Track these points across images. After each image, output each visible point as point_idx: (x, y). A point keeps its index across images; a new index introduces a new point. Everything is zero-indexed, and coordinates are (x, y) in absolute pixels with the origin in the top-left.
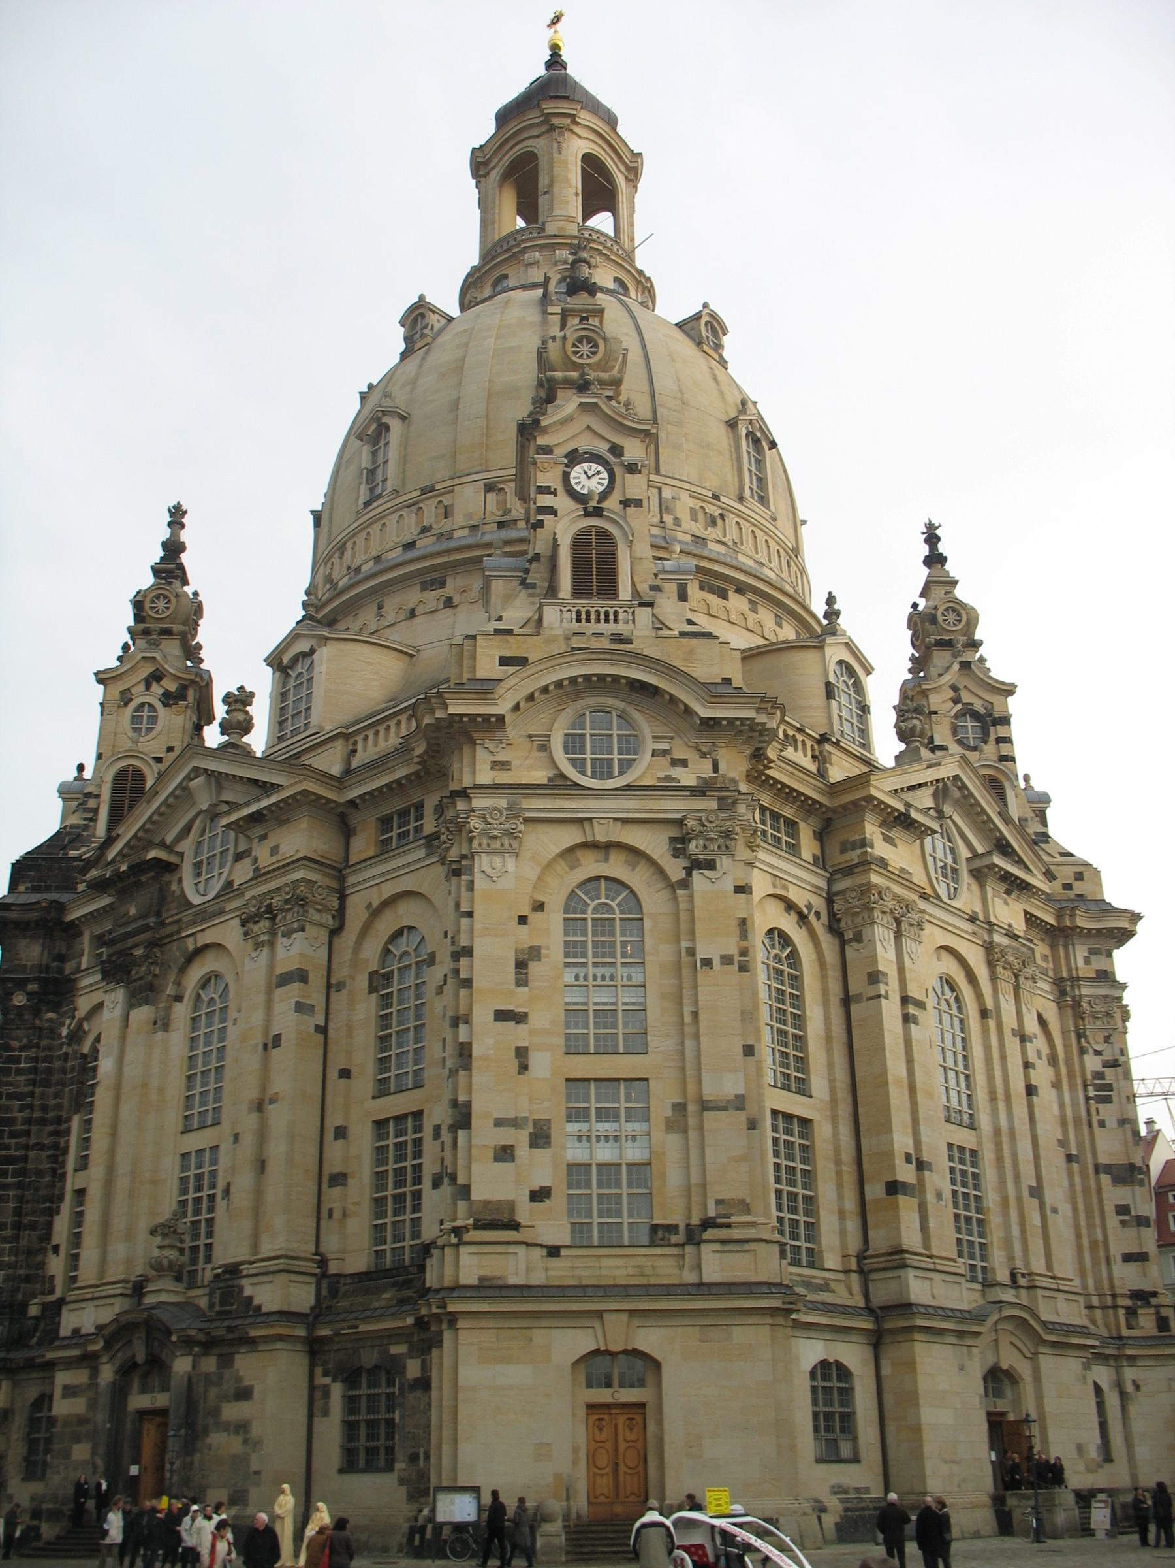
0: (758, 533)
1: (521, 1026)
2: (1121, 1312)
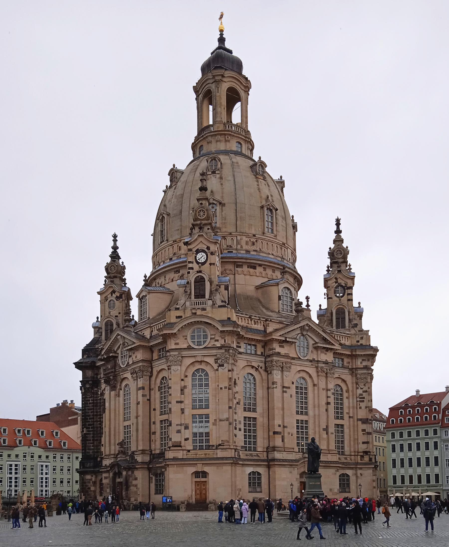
0: (269, 243)
1: (182, 404)
2: (359, 457)
